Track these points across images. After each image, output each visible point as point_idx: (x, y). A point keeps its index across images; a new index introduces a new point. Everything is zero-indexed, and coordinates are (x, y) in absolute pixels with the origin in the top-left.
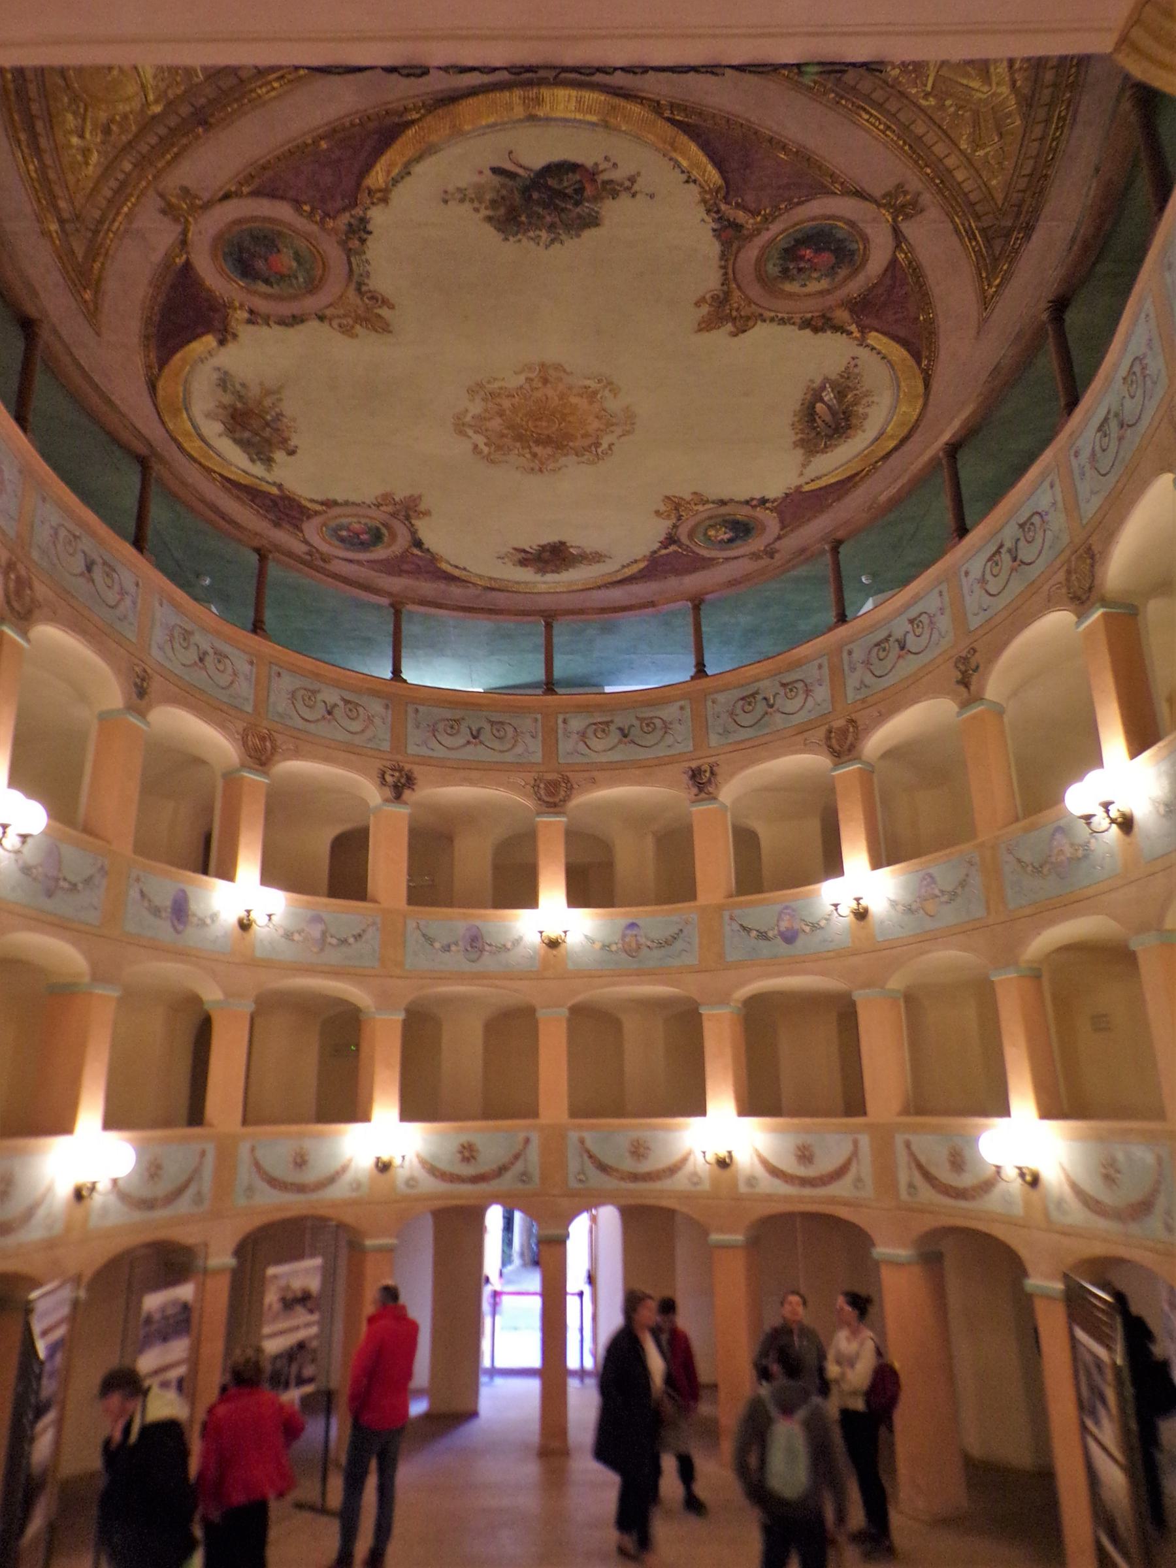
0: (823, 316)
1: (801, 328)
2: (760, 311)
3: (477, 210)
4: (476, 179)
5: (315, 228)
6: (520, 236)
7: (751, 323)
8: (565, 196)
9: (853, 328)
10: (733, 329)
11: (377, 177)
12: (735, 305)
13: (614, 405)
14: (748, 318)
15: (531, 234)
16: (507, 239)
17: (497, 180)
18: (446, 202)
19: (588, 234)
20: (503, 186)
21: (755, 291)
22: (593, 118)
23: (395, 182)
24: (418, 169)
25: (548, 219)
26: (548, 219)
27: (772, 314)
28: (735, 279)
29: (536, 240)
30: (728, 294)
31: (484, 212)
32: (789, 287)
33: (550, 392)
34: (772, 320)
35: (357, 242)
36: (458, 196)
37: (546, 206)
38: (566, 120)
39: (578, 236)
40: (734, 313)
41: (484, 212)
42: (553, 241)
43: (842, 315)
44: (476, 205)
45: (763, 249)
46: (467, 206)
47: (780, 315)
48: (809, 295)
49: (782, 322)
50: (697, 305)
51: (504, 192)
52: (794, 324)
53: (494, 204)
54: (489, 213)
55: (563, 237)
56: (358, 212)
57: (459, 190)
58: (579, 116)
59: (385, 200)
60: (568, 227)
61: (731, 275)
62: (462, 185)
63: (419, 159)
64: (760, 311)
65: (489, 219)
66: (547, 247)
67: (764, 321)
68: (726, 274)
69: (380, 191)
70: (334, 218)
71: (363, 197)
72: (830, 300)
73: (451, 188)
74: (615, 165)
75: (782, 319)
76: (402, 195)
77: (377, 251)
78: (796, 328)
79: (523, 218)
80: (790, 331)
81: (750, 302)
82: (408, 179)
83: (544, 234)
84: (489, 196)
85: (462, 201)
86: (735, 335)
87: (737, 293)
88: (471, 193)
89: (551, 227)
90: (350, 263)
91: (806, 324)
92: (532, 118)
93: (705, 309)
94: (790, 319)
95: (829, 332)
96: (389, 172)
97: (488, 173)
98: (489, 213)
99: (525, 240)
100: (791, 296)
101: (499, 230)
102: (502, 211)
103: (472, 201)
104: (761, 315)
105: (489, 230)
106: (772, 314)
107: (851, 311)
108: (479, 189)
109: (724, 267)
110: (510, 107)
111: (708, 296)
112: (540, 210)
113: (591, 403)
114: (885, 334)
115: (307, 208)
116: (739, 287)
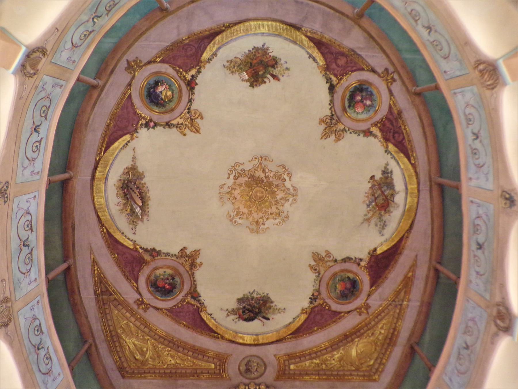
0: (154, 257)
1: (160, 251)
2: (178, 260)
3: (275, 306)
4: (274, 317)
5: (326, 301)
6: (263, 295)
7: (180, 254)
8: (248, 310)
9: (141, 251)
10: (186, 251)
11: (303, 317)
12: (187, 263)
13: (229, 207)
14: (181, 256)
15: (259, 296)
16: (267, 294)
17: (268, 316)
18: (284, 309)
19: (241, 296)
20: (267, 314)
21: (181, 270)
22: (240, 335)
23: (298, 316)
24: (291, 320)
25: (253, 302)
26: (253, 302)
27: (172, 258)
28: (189, 275)
29: (258, 294)
30: (191, 269)
31: (273, 305)
32: (169, 271)
33: (255, 215)
34: (172, 255)
35: (315, 294)
36: (280, 311)
37: (254, 306)
38: (248, 334)
39: (244, 295)
40: (187, 259)
41: (273, 305)
42: (252, 293)
43: (147, 257)
44: (275, 308)
45: (182, 289)
46: (278, 307)
47: (170, 258)
48: (162, 267)
49: (168, 254)
50: (201, 264)
51: (267, 312)
52: (164, 253)
53: (270, 308)
54: (272, 305)
55: (249, 295)
56: (312, 306)
57: (280, 313)
58: (244, 335)
59: (303, 310)
60: (247, 298)
61: (192, 277)
62: (279, 314)
63: (290, 323)
64: (178, 260)
65: (272, 302)
66: (254, 291)
67: (175, 255)
68: (194, 278)
69: (303, 313)
70: (320, 304)
71: (309, 310)
72: (153, 265)
73: (282, 313)
74: (233, 320)
75: (169, 256)
76: (299, 311)
77: (309, 291)
78: (163, 251)
79: (261, 302)
80: (164, 250)
81: (182, 264)
82: (294, 317)
83: (255, 296)
84: (271, 311)
85: (279, 309)
86: (185, 248)
87: (188, 269)
88: (277, 312)
89: (252, 299)
90: (319, 286)
91: (159, 253)
92: (257, 335)
93: (198, 261)
94: (166, 256)
95: (149, 248)
96: (299, 319)
97: (271, 319)
98: (272, 305)
99: (261, 294)
100: (169, 267)
101: (269, 298)
102: (268, 305)
103: (277, 309)
104: (177, 258)
105: (273, 298)
106: (172, 258)
107: (144, 259)
108: (274, 313)
109: (195, 281)
110: (263, 339)
111: (198, 268)
112: (256, 305)
113: (239, 208)
114: (128, 248)
115: (327, 308)
116: (188, 272)
